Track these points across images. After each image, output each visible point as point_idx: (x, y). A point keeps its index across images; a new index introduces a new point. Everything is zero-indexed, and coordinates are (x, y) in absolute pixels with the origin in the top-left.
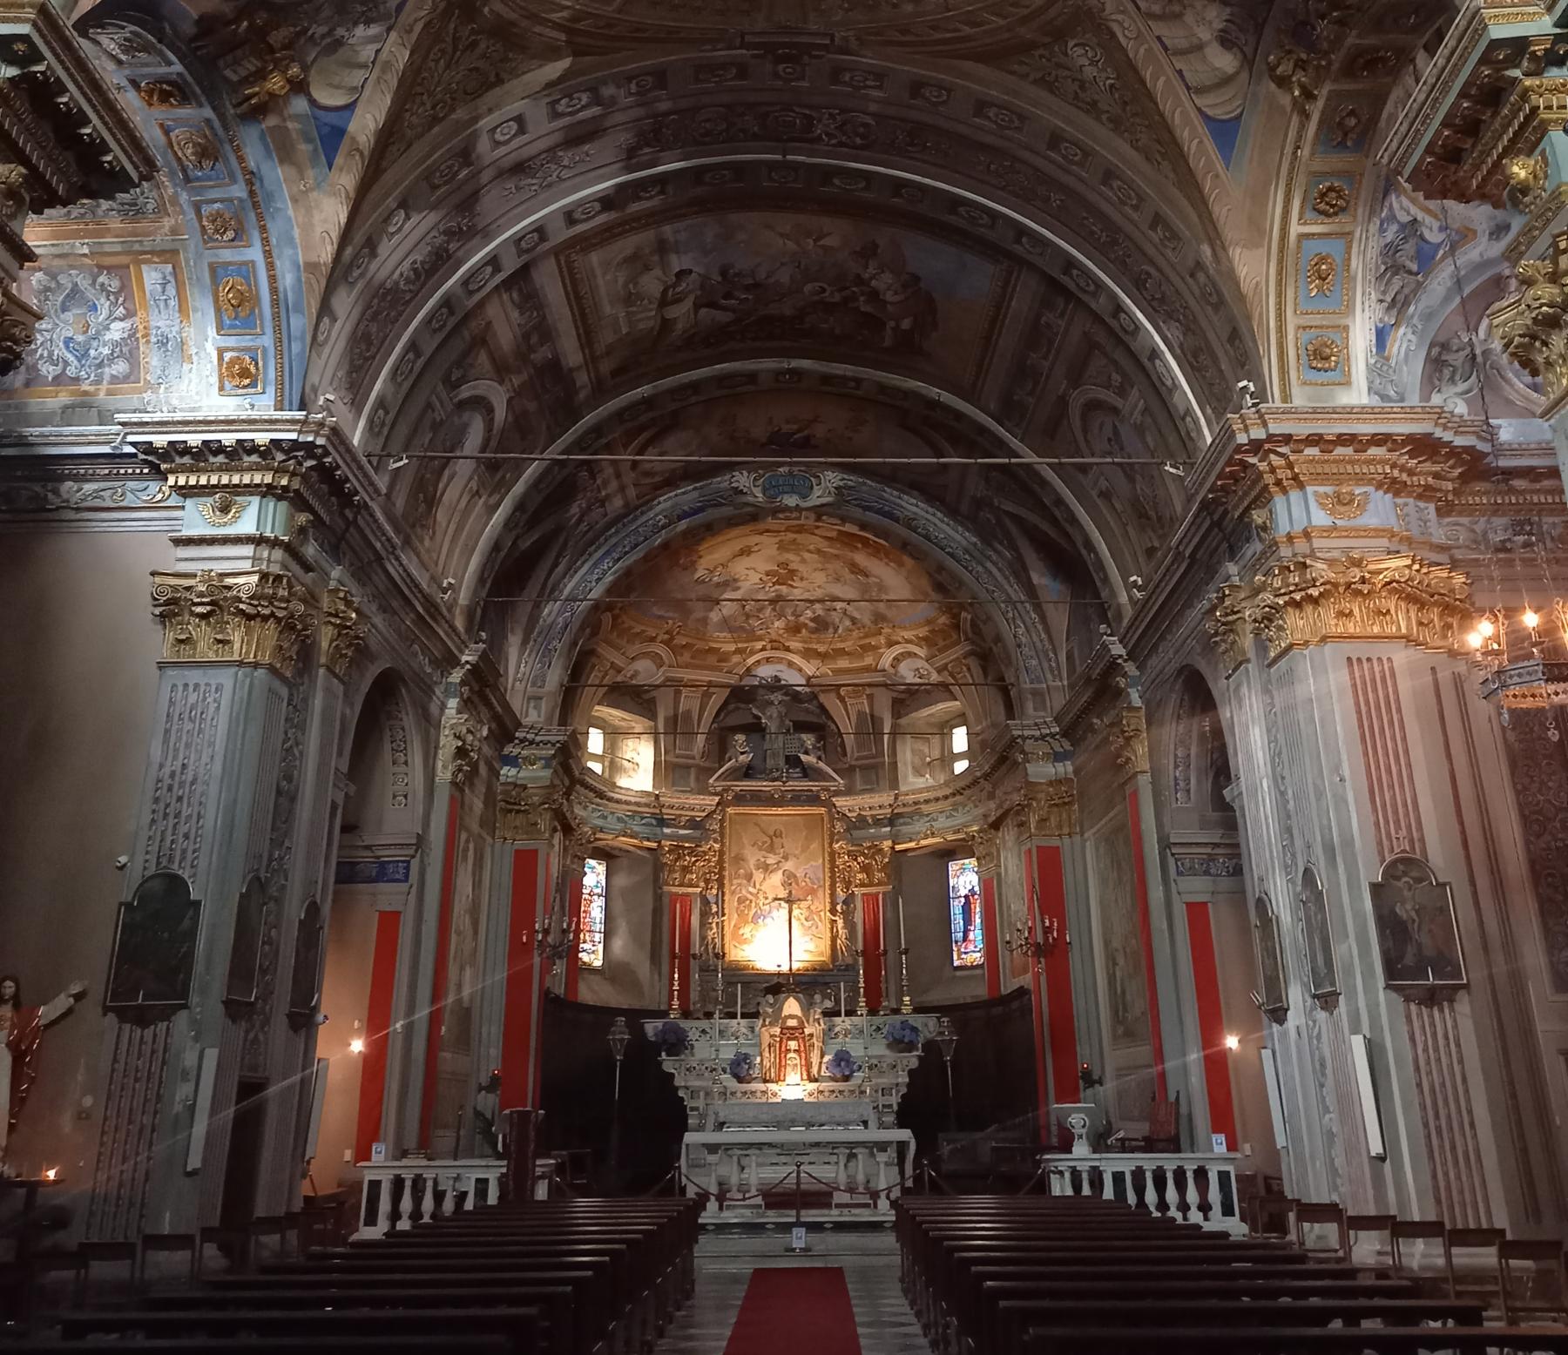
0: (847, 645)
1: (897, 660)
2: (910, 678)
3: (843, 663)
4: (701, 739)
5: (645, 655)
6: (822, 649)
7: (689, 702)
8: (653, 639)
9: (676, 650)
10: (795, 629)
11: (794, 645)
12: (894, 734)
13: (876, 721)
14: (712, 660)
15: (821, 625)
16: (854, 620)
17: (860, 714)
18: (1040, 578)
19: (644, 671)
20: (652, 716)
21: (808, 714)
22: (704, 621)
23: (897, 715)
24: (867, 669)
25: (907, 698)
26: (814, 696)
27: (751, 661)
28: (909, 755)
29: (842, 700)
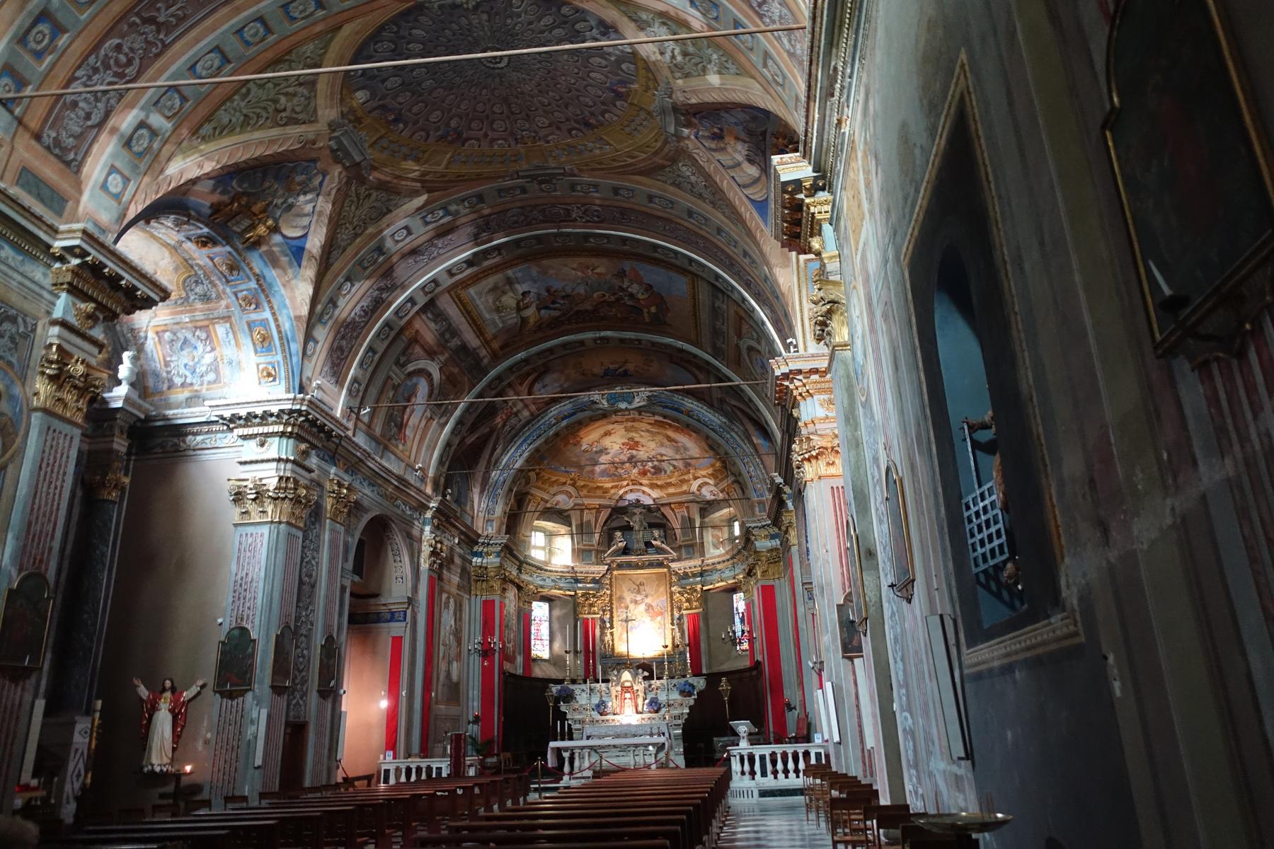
0: (673, 480)
2: (709, 497)
3: (671, 490)
4: (597, 536)
8: (564, 484)
10: (644, 473)
11: (644, 482)
12: (701, 527)
13: (691, 521)
14: (599, 493)
16: (674, 467)
17: (683, 517)
19: (562, 501)
20: (570, 525)
21: (656, 518)
22: (593, 472)
23: (702, 516)
24: (684, 493)
25: (707, 507)
27: (621, 492)
28: (710, 538)
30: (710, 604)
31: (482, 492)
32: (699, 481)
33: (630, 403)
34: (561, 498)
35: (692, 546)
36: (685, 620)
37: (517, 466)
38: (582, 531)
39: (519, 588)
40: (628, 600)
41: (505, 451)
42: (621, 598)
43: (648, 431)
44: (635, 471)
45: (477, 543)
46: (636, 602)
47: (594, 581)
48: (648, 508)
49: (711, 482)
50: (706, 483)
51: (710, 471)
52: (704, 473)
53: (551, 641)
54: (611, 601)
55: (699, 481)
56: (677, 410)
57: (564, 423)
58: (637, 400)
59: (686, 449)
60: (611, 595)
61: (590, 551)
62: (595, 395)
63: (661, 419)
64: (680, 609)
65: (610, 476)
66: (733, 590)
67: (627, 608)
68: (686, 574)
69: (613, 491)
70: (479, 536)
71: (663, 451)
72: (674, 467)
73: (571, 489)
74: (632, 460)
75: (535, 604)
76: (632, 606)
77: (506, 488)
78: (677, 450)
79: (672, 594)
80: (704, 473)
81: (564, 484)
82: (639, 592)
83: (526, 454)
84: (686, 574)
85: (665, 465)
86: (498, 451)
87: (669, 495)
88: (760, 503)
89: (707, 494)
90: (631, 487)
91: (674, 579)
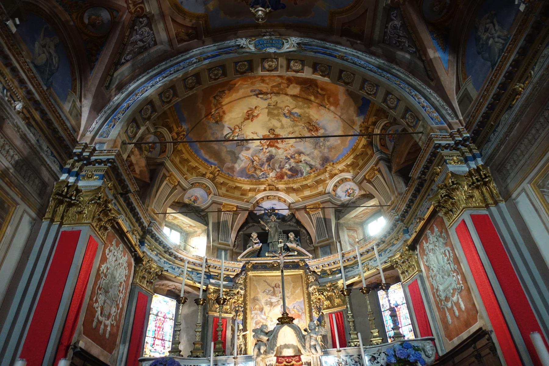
0: (309, 182)
1: (336, 186)
2: (344, 198)
3: (307, 193)
4: (233, 236)
5: (201, 185)
6: (295, 186)
7: (225, 217)
8: (204, 175)
9: (218, 185)
10: (280, 177)
11: (281, 186)
12: (337, 226)
13: (327, 221)
14: (237, 194)
15: (295, 172)
16: (311, 167)
17: (318, 219)
18: (435, 53)
20: (207, 224)
21: (291, 225)
22: (232, 169)
23: (338, 218)
24: (320, 194)
25: (342, 209)
26: (293, 215)
27: (259, 196)
28: (346, 238)
29: (308, 213)
31: (97, 108)
32: (336, 179)
34: (198, 192)
36: (327, 320)
37: (146, 94)
38: (220, 228)
39: (138, 260)
40: (263, 302)
42: (255, 300)
44: (272, 174)
45: (71, 155)
46: (271, 304)
47: (227, 278)
48: (283, 219)
49: (348, 176)
51: (349, 161)
52: (341, 166)
54: (245, 302)
55: (336, 179)
60: (245, 296)
62: (243, 42)
63: (307, 73)
64: (319, 309)
65: (249, 176)
66: (375, 286)
67: (262, 310)
68: (324, 272)
69: (250, 194)
72: (311, 167)
73: (209, 184)
74: (271, 158)
76: (267, 308)
77: (129, 112)
79: (309, 295)
80: (341, 166)
81: (204, 175)
84: (324, 272)
85: (302, 166)
86: (125, 70)
87: (304, 198)
89: (342, 196)
90: (267, 193)
91: (312, 279)
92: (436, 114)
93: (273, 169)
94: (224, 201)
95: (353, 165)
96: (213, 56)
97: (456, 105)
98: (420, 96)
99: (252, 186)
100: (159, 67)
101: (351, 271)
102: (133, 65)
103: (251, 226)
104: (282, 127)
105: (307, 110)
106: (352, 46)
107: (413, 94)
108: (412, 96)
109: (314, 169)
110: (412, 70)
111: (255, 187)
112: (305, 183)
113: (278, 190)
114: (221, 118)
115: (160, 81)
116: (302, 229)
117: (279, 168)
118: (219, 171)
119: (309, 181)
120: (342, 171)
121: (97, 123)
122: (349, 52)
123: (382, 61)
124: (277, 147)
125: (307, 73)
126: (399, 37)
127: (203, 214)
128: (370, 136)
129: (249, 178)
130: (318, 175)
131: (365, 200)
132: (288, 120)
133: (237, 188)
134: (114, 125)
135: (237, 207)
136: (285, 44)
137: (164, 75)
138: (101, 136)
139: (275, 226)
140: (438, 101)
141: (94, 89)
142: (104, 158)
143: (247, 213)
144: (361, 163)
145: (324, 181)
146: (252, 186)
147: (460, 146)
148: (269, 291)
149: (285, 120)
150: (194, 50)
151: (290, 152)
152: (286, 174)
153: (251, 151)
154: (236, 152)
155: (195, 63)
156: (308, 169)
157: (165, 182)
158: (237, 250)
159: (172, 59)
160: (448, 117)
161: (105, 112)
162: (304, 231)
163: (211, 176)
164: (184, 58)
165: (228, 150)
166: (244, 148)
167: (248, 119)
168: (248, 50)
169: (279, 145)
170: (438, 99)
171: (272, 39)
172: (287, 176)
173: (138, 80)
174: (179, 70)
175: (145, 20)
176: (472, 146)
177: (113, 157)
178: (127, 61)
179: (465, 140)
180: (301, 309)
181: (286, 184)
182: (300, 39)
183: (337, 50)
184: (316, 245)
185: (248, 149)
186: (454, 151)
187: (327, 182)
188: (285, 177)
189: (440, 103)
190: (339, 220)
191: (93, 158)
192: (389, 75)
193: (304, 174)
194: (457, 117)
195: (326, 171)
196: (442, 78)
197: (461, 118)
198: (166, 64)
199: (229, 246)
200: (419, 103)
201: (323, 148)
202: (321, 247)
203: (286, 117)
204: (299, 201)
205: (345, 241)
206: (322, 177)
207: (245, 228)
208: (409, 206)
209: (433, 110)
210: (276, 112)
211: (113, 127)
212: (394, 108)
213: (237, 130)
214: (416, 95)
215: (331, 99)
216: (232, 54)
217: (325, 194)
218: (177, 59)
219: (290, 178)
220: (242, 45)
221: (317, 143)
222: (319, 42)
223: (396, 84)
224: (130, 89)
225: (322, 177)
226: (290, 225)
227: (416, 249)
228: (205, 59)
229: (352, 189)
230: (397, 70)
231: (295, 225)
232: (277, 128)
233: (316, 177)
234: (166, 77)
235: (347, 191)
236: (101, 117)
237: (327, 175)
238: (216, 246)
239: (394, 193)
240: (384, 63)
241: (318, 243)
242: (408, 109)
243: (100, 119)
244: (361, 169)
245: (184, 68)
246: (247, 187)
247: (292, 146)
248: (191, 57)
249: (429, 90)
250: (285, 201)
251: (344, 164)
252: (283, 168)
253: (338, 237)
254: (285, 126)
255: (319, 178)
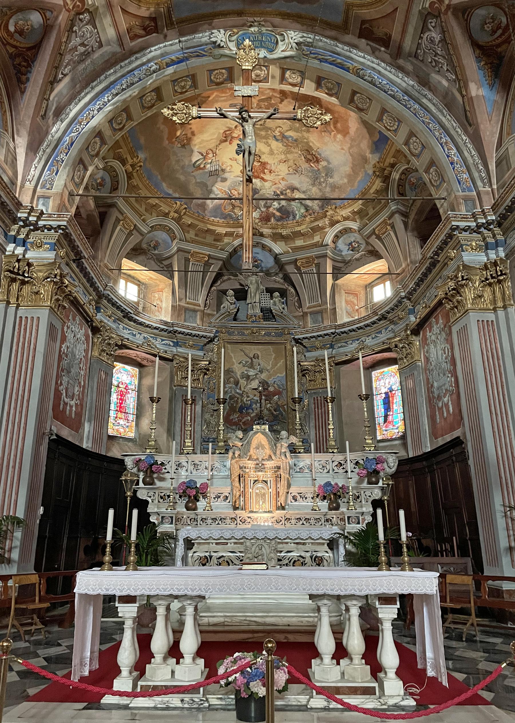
0: (302, 228)
3: (299, 243)
6: (284, 232)
8: (166, 215)
9: (185, 228)
11: (266, 231)
14: (209, 239)
15: (285, 214)
18: (480, 89)
22: (203, 206)
23: (336, 278)
28: (344, 304)
30: (343, 382)
31: (33, 148)
32: (338, 227)
33: (271, 51)
35: (321, 312)
37: (93, 123)
41: (73, 97)
43: (283, 138)
49: (354, 225)
50: (346, 231)
51: (357, 206)
52: (345, 212)
53: (139, 416)
55: (338, 227)
56: (342, 66)
57: (170, 70)
58: (281, 46)
59: (329, 172)
61: (195, 311)
62: (220, 36)
63: (308, 88)
65: (225, 217)
69: (226, 240)
70: (19, 205)
71: (295, 181)
75: (119, 366)
77: (74, 151)
78: (315, 180)
80: (345, 212)
81: (166, 215)
82: (252, 366)
83: (109, 108)
87: (296, 249)
88: (466, 199)
92: (465, 176)
93: (257, 207)
94: (193, 248)
95: (361, 214)
96: (180, 61)
97: (492, 167)
98: (452, 146)
99: (229, 230)
100: (106, 78)
101: (345, 346)
102: (72, 80)
103: (227, 280)
104: (272, 153)
105: (305, 135)
106: (374, 52)
107: (444, 140)
108: (441, 144)
109: (311, 212)
110: (449, 104)
111: (232, 230)
112: (298, 229)
113: (262, 235)
114: (189, 140)
115: (109, 101)
116: (290, 288)
117: (265, 206)
118: (185, 208)
119: (303, 227)
120: (346, 219)
121: (36, 167)
122: (369, 63)
123: (411, 83)
124: (263, 179)
125: (308, 88)
126: (436, 54)
127: (166, 263)
128: (386, 179)
129: (224, 218)
130: (316, 220)
131: (372, 258)
132: (280, 145)
133: (208, 231)
134: (58, 171)
135: (209, 256)
136: (280, 43)
137: (114, 91)
138: (43, 187)
139: (257, 282)
140: (472, 157)
141: (28, 122)
142: (54, 224)
143: (221, 263)
144: (371, 212)
145: (323, 228)
146: (229, 230)
147: (482, 229)
148: (246, 362)
149: (275, 145)
150: (153, 49)
151: (280, 186)
152: (274, 214)
153: (228, 183)
154: (208, 183)
155: (154, 72)
156: (303, 211)
157: (119, 228)
158: (209, 311)
159: (123, 64)
160: (479, 184)
161: (44, 151)
162: (292, 290)
163: (176, 215)
164: (138, 62)
165: (198, 181)
166: (219, 179)
167: (226, 141)
168: (227, 52)
169: (265, 177)
170: (473, 153)
171: (260, 33)
172: (275, 218)
173: (80, 101)
174: (133, 84)
175: (86, 16)
176: (497, 230)
177: (65, 223)
178: (65, 75)
179: (489, 223)
180: (283, 385)
181: (273, 228)
182: (301, 35)
183: (352, 59)
184: (306, 310)
185: (224, 180)
186: (475, 234)
187: (326, 230)
188: (272, 219)
189: (474, 160)
190: (336, 280)
191: (41, 223)
192: (417, 106)
193: (297, 217)
194: (491, 185)
195: (326, 217)
196: (482, 127)
197: (495, 187)
198: (115, 72)
199: (200, 306)
200: (448, 156)
201: (324, 185)
202: (311, 313)
203: (277, 140)
204: (288, 252)
205: (341, 309)
206: (320, 223)
207: (219, 282)
208: (418, 285)
209: (464, 169)
210: (263, 133)
211: (56, 174)
212: (417, 156)
213: (211, 155)
214: (446, 143)
215: (339, 125)
216: (205, 58)
217: (322, 245)
218: (130, 63)
219: (278, 220)
220: (219, 42)
221: (317, 178)
222: (328, 41)
223: (423, 122)
224: (72, 115)
225: (320, 223)
226: (275, 281)
227: (419, 334)
228: (168, 65)
229: (358, 242)
230: (430, 100)
231: (282, 281)
232: (264, 153)
233: (312, 222)
234: (117, 94)
235: (351, 244)
236: (40, 159)
237: (327, 221)
238: (183, 307)
239: (406, 259)
240: (413, 86)
241: (308, 308)
242: (432, 163)
243: (39, 162)
244: (370, 220)
245: (140, 80)
246: (222, 230)
247: (283, 179)
248: (149, 61)
249: (464, 138)
250: (270, 250)
251: (350, 209)
252: (270, 207)
253: (334, 302)
254: (275, 152)
255: (316, 223)
